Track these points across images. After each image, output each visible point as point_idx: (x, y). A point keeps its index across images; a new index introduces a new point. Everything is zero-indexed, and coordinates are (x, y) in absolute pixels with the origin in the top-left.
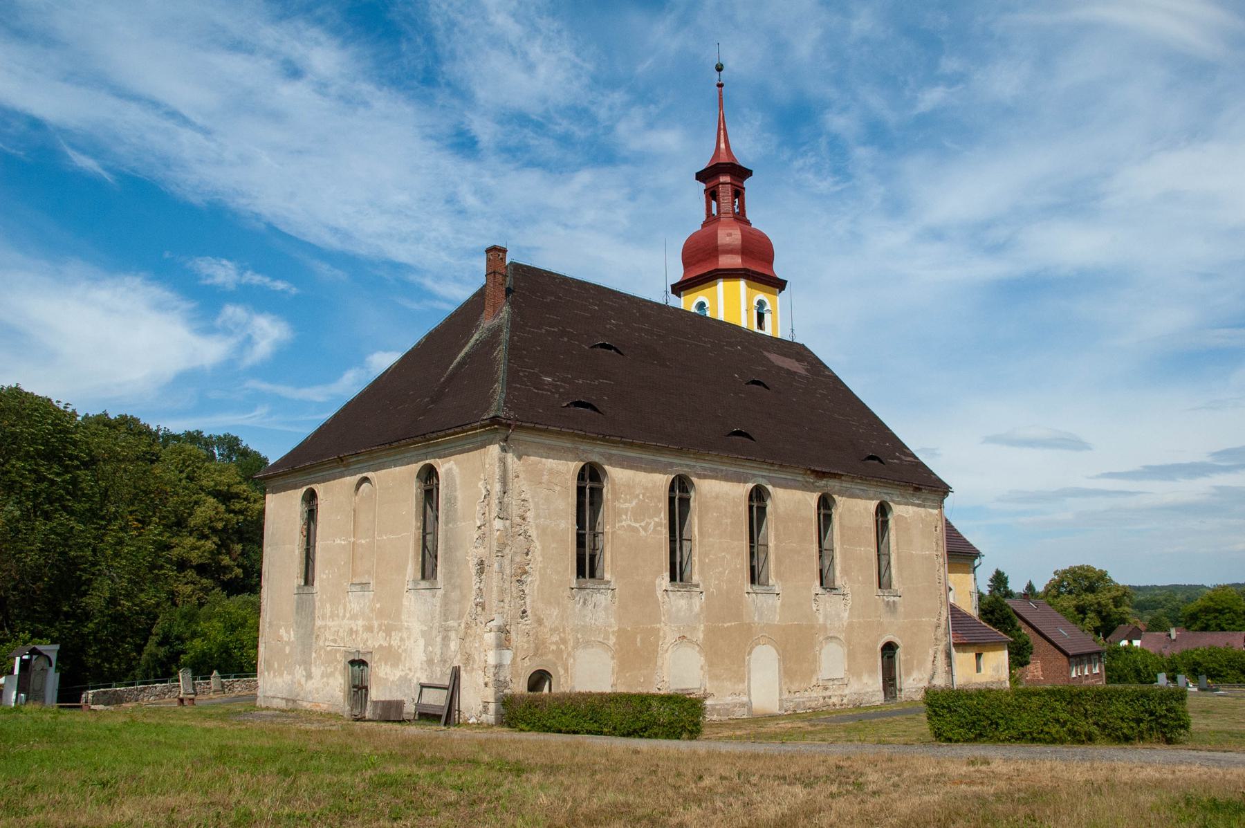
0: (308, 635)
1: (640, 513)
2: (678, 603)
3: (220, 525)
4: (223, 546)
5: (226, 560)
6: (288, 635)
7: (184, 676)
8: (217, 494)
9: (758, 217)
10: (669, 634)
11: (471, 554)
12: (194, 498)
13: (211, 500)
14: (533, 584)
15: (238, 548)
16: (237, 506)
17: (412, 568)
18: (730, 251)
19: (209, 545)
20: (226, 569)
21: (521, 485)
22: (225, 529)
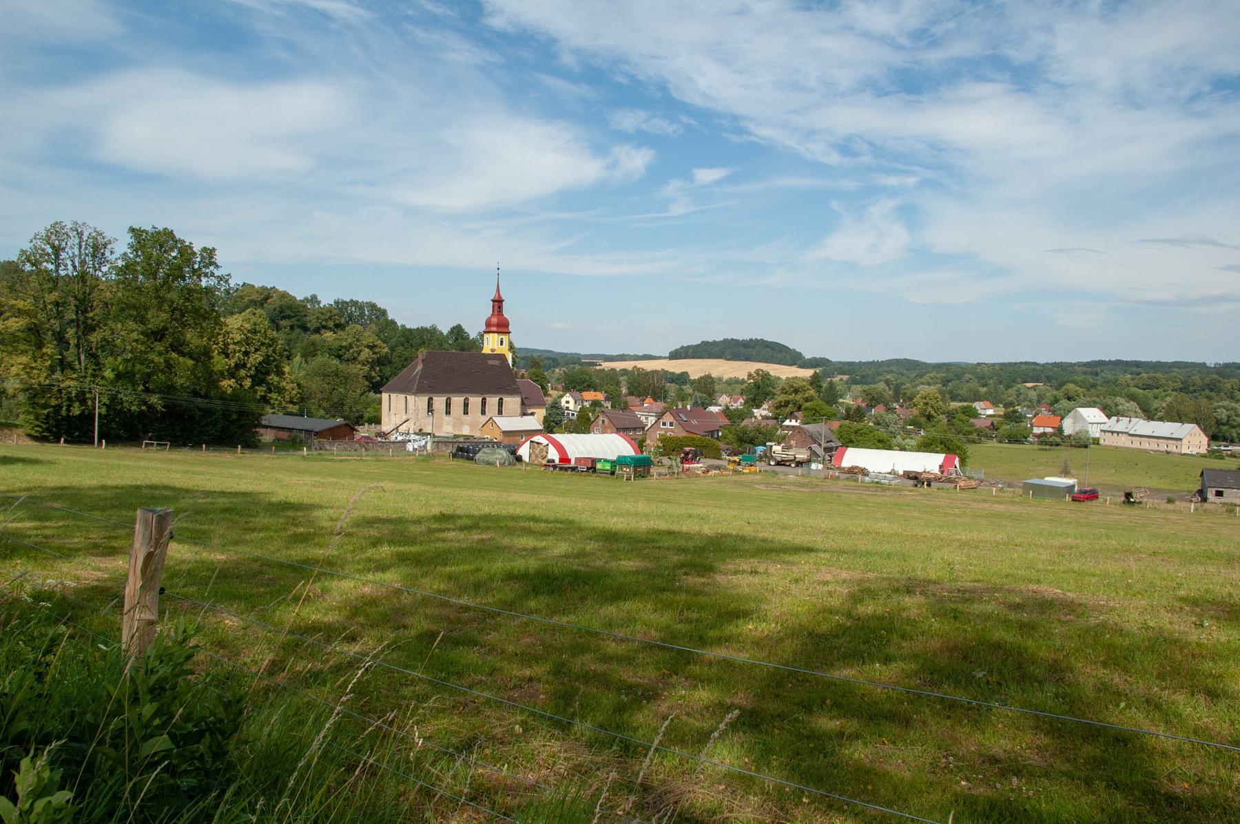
0: (390, 420)
1: (440, 404)
2: (447, 418)
3: (370, 360)
4: (372, 368)
5: (373, 374)
6: (387, 420)
7: (366, 424)
8: (368, 346)
9: (506, 313)
10: (445, 423)
11: (411, 411)
12: (360, 348)
13: (367, 350)
14: (419, 417)
15: (378, 368)
16: (377, 350)
17: (404, 412)
18: (494, 325)
19: (367, 368)
20: (374, 378)
21: (418, 402)
22: (373, 361)
